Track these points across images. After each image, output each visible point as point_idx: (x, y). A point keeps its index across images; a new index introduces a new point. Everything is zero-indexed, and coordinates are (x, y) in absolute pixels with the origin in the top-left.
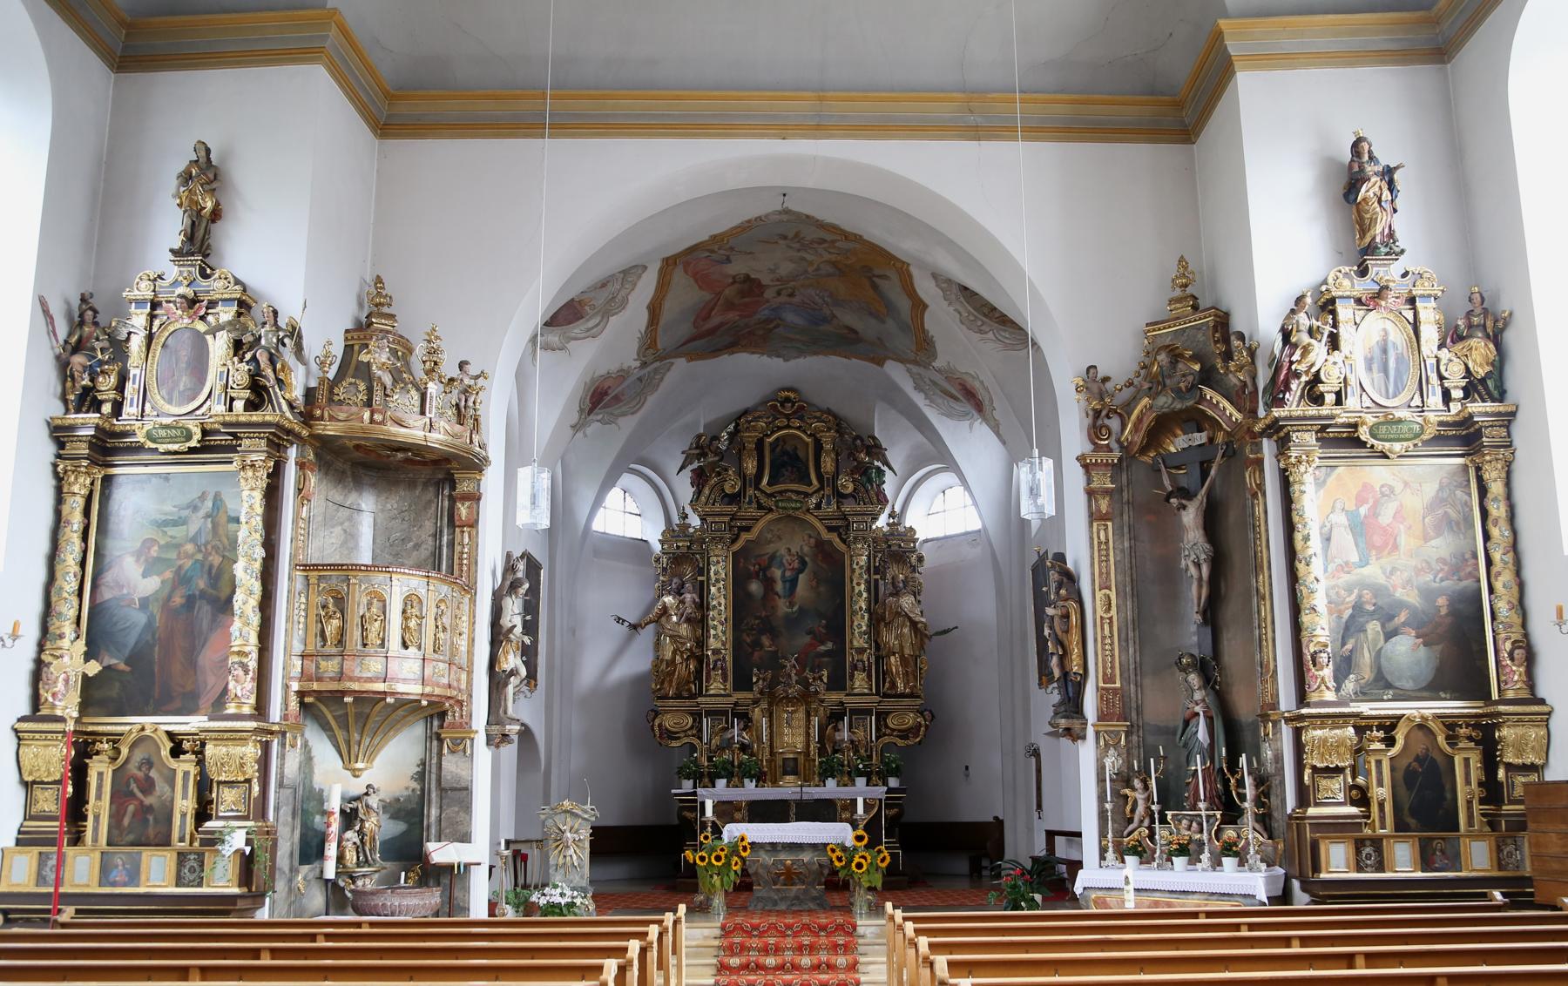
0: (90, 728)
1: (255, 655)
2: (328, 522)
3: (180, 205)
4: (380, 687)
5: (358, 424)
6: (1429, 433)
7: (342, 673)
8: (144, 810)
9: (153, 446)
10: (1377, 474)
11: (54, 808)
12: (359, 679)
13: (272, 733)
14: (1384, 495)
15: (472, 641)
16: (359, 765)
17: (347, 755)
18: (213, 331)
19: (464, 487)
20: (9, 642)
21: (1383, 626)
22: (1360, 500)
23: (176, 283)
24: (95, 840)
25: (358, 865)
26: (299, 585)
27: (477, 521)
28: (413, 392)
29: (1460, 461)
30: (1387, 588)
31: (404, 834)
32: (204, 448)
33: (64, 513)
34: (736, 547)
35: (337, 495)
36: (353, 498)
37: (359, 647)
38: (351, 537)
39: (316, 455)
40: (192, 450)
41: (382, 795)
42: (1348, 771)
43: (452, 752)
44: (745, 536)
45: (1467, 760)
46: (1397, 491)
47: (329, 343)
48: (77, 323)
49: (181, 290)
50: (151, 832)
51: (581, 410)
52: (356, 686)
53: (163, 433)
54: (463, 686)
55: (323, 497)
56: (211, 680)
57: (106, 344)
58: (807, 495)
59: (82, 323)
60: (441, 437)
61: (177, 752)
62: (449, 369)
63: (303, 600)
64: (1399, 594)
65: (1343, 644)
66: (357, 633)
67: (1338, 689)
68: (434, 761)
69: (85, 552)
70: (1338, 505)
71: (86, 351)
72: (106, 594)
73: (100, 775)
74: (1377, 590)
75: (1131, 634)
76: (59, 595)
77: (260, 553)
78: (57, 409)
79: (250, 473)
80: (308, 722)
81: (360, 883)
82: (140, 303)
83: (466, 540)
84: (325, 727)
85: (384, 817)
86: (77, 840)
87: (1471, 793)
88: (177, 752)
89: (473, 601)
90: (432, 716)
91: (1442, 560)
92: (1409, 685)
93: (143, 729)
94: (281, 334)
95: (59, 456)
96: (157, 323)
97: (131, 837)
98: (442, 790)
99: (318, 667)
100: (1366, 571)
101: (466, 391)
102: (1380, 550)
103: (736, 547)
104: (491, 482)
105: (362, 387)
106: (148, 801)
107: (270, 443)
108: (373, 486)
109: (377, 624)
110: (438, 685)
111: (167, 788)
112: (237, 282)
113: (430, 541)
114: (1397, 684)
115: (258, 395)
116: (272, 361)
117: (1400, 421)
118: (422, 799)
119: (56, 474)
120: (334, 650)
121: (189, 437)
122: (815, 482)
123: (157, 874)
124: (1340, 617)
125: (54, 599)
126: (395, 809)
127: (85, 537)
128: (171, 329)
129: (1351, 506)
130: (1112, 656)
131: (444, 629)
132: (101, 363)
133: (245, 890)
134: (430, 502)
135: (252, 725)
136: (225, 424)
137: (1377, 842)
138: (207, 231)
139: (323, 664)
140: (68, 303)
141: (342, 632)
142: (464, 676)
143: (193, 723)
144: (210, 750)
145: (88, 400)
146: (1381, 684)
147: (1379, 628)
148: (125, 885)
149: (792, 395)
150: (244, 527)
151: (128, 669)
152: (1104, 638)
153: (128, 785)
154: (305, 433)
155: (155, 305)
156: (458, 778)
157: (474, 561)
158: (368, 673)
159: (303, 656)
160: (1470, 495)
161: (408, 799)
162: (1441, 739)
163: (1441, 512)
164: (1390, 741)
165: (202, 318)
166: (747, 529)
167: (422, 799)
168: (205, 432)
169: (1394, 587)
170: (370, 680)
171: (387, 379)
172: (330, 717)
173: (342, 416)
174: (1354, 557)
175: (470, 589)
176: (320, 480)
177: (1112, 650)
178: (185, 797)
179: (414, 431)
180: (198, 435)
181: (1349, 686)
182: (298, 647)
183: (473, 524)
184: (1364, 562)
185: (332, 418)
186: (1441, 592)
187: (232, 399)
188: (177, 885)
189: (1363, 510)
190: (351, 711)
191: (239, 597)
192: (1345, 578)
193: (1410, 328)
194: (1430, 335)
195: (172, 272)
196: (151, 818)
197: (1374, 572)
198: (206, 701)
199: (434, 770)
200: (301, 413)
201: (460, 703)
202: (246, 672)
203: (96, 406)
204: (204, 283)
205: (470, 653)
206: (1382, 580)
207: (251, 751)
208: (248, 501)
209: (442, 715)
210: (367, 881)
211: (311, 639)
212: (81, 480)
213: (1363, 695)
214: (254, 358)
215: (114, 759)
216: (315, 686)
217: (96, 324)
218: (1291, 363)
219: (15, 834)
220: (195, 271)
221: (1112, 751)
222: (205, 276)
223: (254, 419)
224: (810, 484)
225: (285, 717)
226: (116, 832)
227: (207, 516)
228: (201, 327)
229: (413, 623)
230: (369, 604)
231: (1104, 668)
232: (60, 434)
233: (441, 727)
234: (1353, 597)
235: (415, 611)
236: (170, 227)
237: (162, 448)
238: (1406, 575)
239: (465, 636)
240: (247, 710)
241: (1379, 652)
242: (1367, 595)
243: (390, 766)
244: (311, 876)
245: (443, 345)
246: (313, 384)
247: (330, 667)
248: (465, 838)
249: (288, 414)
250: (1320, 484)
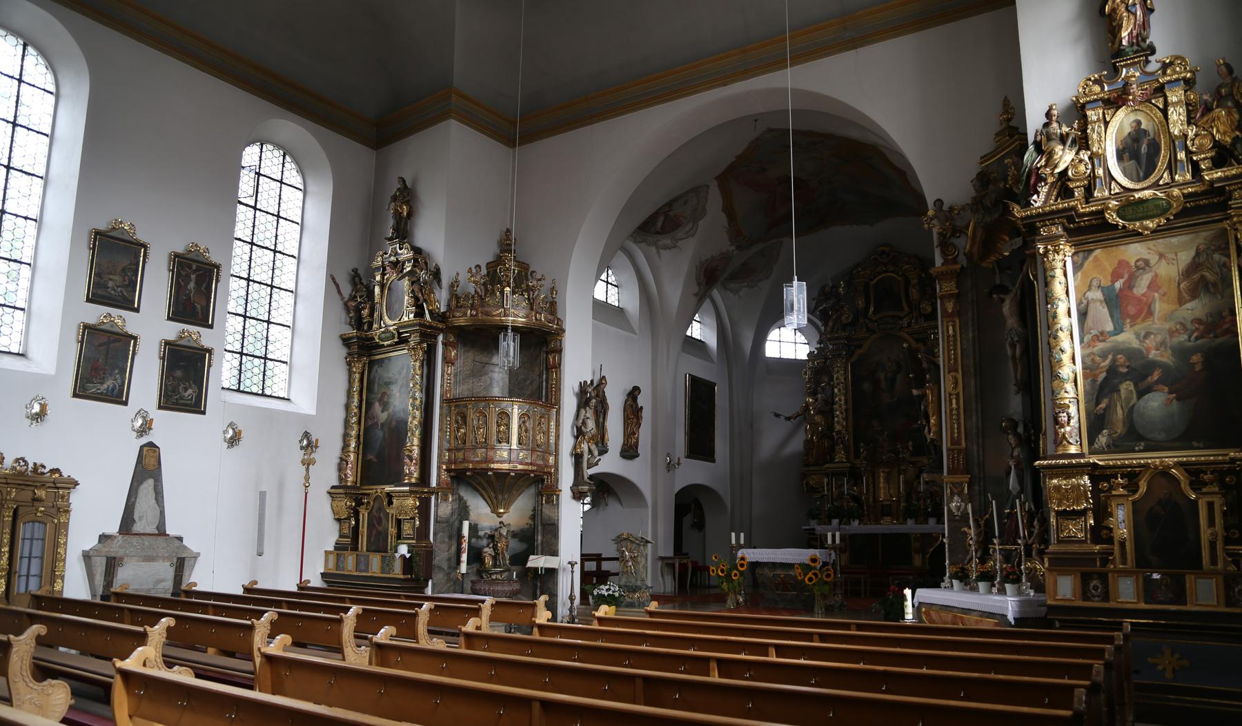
6: (1176, 207)
8: (379, 533)
10: (1134, 251)
14: (1138, 268)
21: (1136, 385)
22: (1116, 276)
29: (1220, 225)
30: (1140, 351)
34: (854, 359)
42: (1090, 514)
44: (859, 351)
45: (1210, 505)
46: (1152, 262)
51: (699, 284)
58: (901, 318)
64: (1153, 355)
65: (1098, 403)
67: (1091, 443)
69: (361, 401)
70: (1095, 283)
74: (1131, 354)
75: (974, 406)
87: (1214, 535)
91: (1199, 321)
92: (1160, 436)
100: (1121, 338)
102: (1134, 319)
103: (854, 359)
114: (1149, 436)
117: (1142, 201)
122: (906, 308)
124: (1094, 381)
129: (1106, 282)
130: (959, 424)
137: (1103, 577)
146: (1133, 437)
147: (1132, 388)
149: (886, 249)
152: (951, 410)
156: (550, 518)
159: (449, 450)
160: (1229, 256)
162: (1185, 485)
163: (1196, 276)
164: (1132, 487)
166: (860, 346)
169: (1148, 350)
174: (1109, 327)
177: (958, 419)
181: (1103, 440)
184: (1118, 330)
186: (1193, 351)
189: (1118, 285)
192: (1101, 346)
193: (1160, 114)
194: (1177, 116)
197: (1127, 337)
206: (1135, 344)
213: (1115, 446)
218: (1039, 169)
221: (956, 498)
224: (902, 310)
231: (952, 433)
234: (1108, 362)
238: (1159, 338)
241: (1132, 409)
242: (1121, 359)
243: (516, 513)
247: (460, 455)
248: (555, 553)
250: (1077, 268)
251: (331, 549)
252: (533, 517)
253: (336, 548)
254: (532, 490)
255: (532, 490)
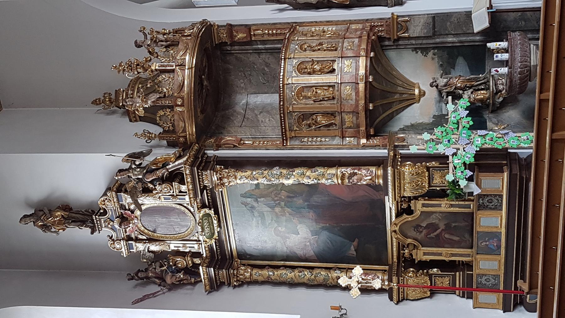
0: (395, 260)
1: (343, 169)
2: (255, 124)
3: (64, 230)
4: (362, 86)
5: (186, 115)
7: (353, 112)
8: (448, 228)
9: (216, 234)
11: (447, 279)
12: (357, 101)
13: (395, 155)
15: (329, 23)
16: (417, 92)
17: (410, 100)
18: (139, 206)
19: (224, 36)
20: (343, 312)
23: (113, 229)
24: (468, 255)
25: (487, 89)
26: (297, 142)
27: (246, 25)
28: (160, 79)
31: (465, 59)
32: (213, 205)
33: (263, 280)
35: (238, 120)
36: (239, 108)
37: (335, 102)
38: (265, 109)
39: (211, 137)
40: (217, 212)
41: (438, 76)
43: (407, 30)
47: (136, 134)
48: (147, 281)
49: (117, 226)
50: (463, 224)
52: (362, 102)
53: (207, 230)
54: (360, 26)
55: (240, 129)
56: (361, 193)
57: (158, 264)
59: (148, 278)
60: (187, 58)
61: (409, 211)
62: (142, 54)
63: (306, 139)
66: (326, 104)
68: (414, 42)
69: (286, 267)
71: (163, 274)
72: (310, 252)
73: (425, 254)
76: (313, 280)
77: (276, 171)
78: (200, 288)
79: (225, 180)
80: (388, 129)
81: (501, 87)
82: (130, 247)
83: (260, 32)
84: (391, 117)
85: (454, 73)
86: (468, 266)
88: (409, 211)
89: (301, 24)
90: (382, 46)
93: (395, 231)
94: (134, 166)
95: (229, 285)
96: (140, 237)
97: (467, 236)
98: (435, 35)
99: (350, 128)
101: (155, 41)
104: (218, 17)
105: (161, 113)
106: (442, 226)
107: (205, 169)
108: (230, 96)
109: (319, 92)
110: (359, 46)
111: (434, 216)
112: (105, 194)
113: (263, 56)
115: (175, 177)
116: (151, 171)
118: (440, 48)
119: (239, 286)
120: (338, 118)
121: (209, 215)
123: (494, 222)
125: (316, 283)
126: (447, 67)
127: (277, 267)
128: (142, 228)
131: (321, 44)
132: (169, 267)
133: (505, 168)
134: (236, 58)
135: (390, 170)
136: (196, 196)
138: (77, 213)
139: (347, 124)
140: (136, 286)
141: (325, 114)
142: (353, 27)
143: (390, 205)
144: (407, 194)
145: (192, 271)
148: (500, 240)
150: (261, 181)
151: (357, 240)
153: (433, 238)
154: (196, 147)
155: (129, 238)
156: (427, 24)
157: (274, 25)
158: (353, 95)
159: (343, 137)
161: (440, 57)
165: (132, 212)
167: (440, 48)
168: (203, 206)
170: (357, 93)
171: (153, 97)
172: (384, 115)
173: (182, 124)
175: (293, 27)
176: (229, 132)
178: (439, 206)
179: (186, 76)
180: (207, 211)
182: (337, 141)
183: (248, 28)
185: (184, 131)
187: (180, 192)
188: (501, 210)
190: (379, 103)
191: (306, 181)
195: (106, 232)
196: (453, 225)
198: (376, 196)
199: (420, 42)
200: (183, 150)
201: (372, 27)
202: (355, 174)
203: (196, 266)
204: (109, 214)
205: (337, 23)
207: (407, 169)
208: (242, 180)
209: (381, 39)
210: (499, 82)
211: (332, 133)
212: (242, 272)
214: (151, 182)
215: (415, 247)
216: (363, 129)
217: (146, 270)
219: (464, 300)
220: (103, 219)
222: (105, 213)
223: (189, 180)
225: (384, 147)
226: (463, 244)
227: (256, 201)
228: (138, 213)
229: (317, 67)
230: (306, 97)
232: (215, 286)
233: (389, 39)
235: (309, 66)
236: (78, 234)
237: (217, 229)
239: (326, 28)
240: (380, 172)
243: (417, 72)
244: (495, 120)
245: (125, 61)
246: (165, 142)
247: (349, 119)
249: (185, 159)
251: (470, 302)
252: (424, 50)
253: (470, 297)
254: (392, 54)
255: (392, 54)
